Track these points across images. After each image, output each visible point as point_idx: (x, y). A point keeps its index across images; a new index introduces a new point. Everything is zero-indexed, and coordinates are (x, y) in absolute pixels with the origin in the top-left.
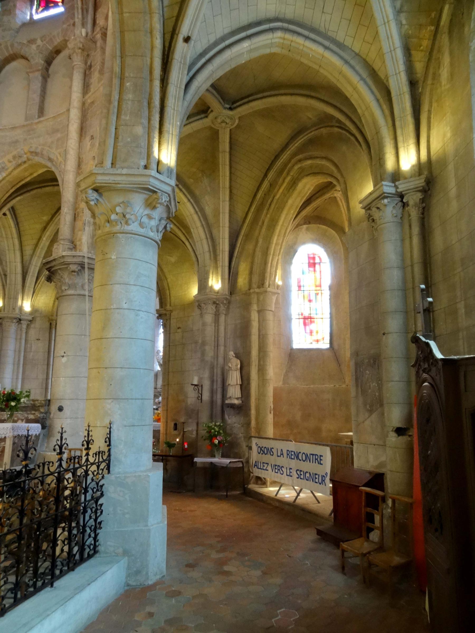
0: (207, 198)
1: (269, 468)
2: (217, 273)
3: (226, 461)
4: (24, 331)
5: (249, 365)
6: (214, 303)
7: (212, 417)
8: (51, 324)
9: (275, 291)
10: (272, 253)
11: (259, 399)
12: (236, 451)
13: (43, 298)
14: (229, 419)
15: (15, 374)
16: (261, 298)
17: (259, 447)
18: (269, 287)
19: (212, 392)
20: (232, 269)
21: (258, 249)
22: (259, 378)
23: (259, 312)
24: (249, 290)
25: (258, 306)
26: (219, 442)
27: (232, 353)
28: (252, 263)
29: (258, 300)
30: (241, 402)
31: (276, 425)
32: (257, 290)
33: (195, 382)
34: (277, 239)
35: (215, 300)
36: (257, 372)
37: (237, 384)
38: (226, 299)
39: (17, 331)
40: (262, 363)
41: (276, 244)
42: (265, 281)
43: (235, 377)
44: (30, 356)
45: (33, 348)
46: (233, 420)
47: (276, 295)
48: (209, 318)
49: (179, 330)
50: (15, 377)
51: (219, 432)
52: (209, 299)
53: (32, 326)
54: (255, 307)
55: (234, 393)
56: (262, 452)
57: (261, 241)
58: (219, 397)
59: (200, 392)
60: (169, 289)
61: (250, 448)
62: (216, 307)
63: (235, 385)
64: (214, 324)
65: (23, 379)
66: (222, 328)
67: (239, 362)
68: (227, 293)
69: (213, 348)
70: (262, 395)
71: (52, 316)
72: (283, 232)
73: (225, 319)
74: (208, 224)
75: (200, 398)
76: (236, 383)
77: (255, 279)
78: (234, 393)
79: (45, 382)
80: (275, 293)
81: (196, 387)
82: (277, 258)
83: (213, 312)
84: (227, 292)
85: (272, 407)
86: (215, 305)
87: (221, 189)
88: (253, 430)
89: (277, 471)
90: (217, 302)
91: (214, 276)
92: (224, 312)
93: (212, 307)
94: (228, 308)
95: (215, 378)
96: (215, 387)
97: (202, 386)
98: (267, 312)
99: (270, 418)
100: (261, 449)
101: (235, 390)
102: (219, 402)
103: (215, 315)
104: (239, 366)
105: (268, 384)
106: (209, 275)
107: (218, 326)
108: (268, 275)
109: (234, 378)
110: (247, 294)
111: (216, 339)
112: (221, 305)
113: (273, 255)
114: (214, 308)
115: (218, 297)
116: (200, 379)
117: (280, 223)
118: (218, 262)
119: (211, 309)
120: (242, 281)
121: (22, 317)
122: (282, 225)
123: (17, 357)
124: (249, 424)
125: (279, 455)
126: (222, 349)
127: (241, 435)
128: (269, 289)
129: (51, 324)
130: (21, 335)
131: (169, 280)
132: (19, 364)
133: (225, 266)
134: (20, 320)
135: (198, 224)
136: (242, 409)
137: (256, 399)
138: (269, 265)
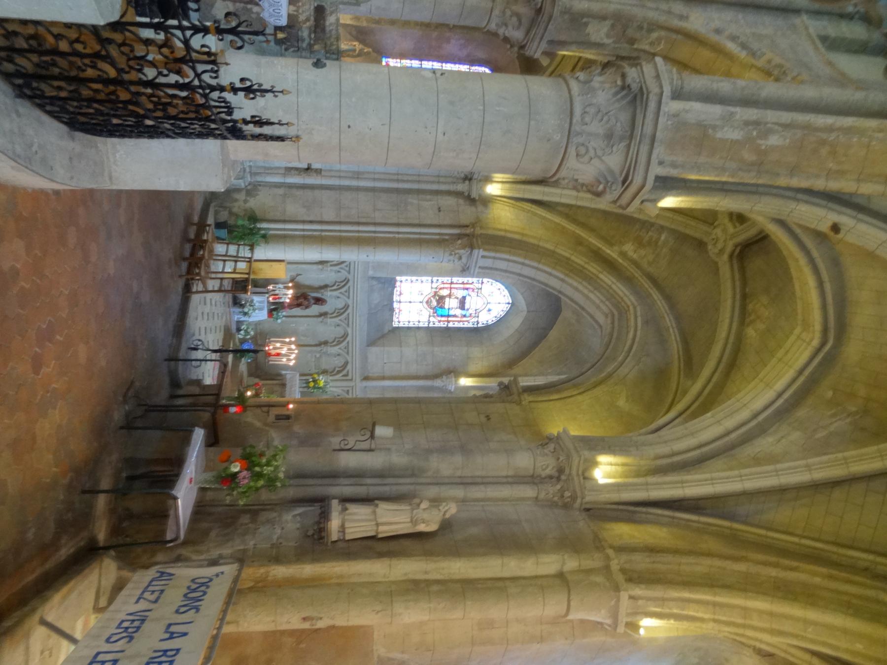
0: (796, 435)
1: (143, 605)
3: (184, 496)
4: (452, 188)
5: (429, 554)
6: (561, 471)
7: (300, 475)
8: (467, 226)
9: (623, 619)
10: (718, 599)
11: (339, 585)
12: (213, 534)
13: (508, 214)
14: (295, 516)
15: (382, 176)
16: (599, 579)
17: (211, 580)
18: (631, 597)
19: (357, 475)
20: (644, 509)
21: (717, 563)
22: (394, 582)
23: (561, 576)
24: (611, 547)
25: (572, 572)
26: (235, 475)
27: (452, 509)
28: (676, 552)
29: (589, 571)
30: (334, 537)
31: (273, 639)
32: (615, 565)
34: (761, 612)
35: (567, 471)
36: (411, 577)
37: (377, 525)
38: (574, 498)
39: (451, 177)
40: (435, 588)
41: (745, 609)
42: (643, 586)
43: (396, 519)
44: (412, 199)
45: (426, 204)
46: (291, 523)
47: (609, 621)
48: (523, 461)
49: (483, 419)
50: (376, 176)
51: (259, 475)
52: (569, 457)
53: (461, 201)
54: (571, 563)
55: (356, 522)
56: (194, 586)
57: (741, 567)
60: (560, 399)
61: (214, 563)
63: (376, 519)
64: (511, 473)
65: (373, 190)
66: (505, 492)
67: (433, 527)
68: (588, 499)
69: (459, 473)
70: (350, 591)
71: (481, 228)
72: (787, 627)
73: (528, 499)
74: (733, 447)
75: (343, 446)
76: (380, 520)
77: (641, 562)
78: (356, 522)
79: (369, 220)
80: (615, 616)
82: (706, 616)
83: (539, 471)
85: (320, 624)
87: (840, 455)
88: (262, 570)
89: (125, 624)
90: (563, 477)
91: (619, 469)
92: (542, 496)
93: (550, 468)
94: (553, 505)
96: (369, 481)
98: (564, 597)
99: (291, 619)
100: (203, 584)
101: (363, 521)
103: (532, 476)
104: (422, 528)
105: (379, 608)
107: (508, 483)
108: (658, 592)
109: (393, 519)
110: (599, 544)
111: (479, 480)
112: (558, 487)
113: (715, 604)
114: (548, 472)
115: (576, 478)
117: (812, 615)
119: (546, 464)
120: (623, 531)
121: (474, 182)
122: (806, 622)
124: (278, 560)
125: (173, 629)
126: (459, 492)
127: (252, 543)
128: (624, 596)
129: (467, 226)
131: (580, 398)
132: (398, 181)
133: (647, 490)
134: (470, 179)
135: (730, 423)
136: (317, 543)
137: (341, 576)
138: (686, 595)
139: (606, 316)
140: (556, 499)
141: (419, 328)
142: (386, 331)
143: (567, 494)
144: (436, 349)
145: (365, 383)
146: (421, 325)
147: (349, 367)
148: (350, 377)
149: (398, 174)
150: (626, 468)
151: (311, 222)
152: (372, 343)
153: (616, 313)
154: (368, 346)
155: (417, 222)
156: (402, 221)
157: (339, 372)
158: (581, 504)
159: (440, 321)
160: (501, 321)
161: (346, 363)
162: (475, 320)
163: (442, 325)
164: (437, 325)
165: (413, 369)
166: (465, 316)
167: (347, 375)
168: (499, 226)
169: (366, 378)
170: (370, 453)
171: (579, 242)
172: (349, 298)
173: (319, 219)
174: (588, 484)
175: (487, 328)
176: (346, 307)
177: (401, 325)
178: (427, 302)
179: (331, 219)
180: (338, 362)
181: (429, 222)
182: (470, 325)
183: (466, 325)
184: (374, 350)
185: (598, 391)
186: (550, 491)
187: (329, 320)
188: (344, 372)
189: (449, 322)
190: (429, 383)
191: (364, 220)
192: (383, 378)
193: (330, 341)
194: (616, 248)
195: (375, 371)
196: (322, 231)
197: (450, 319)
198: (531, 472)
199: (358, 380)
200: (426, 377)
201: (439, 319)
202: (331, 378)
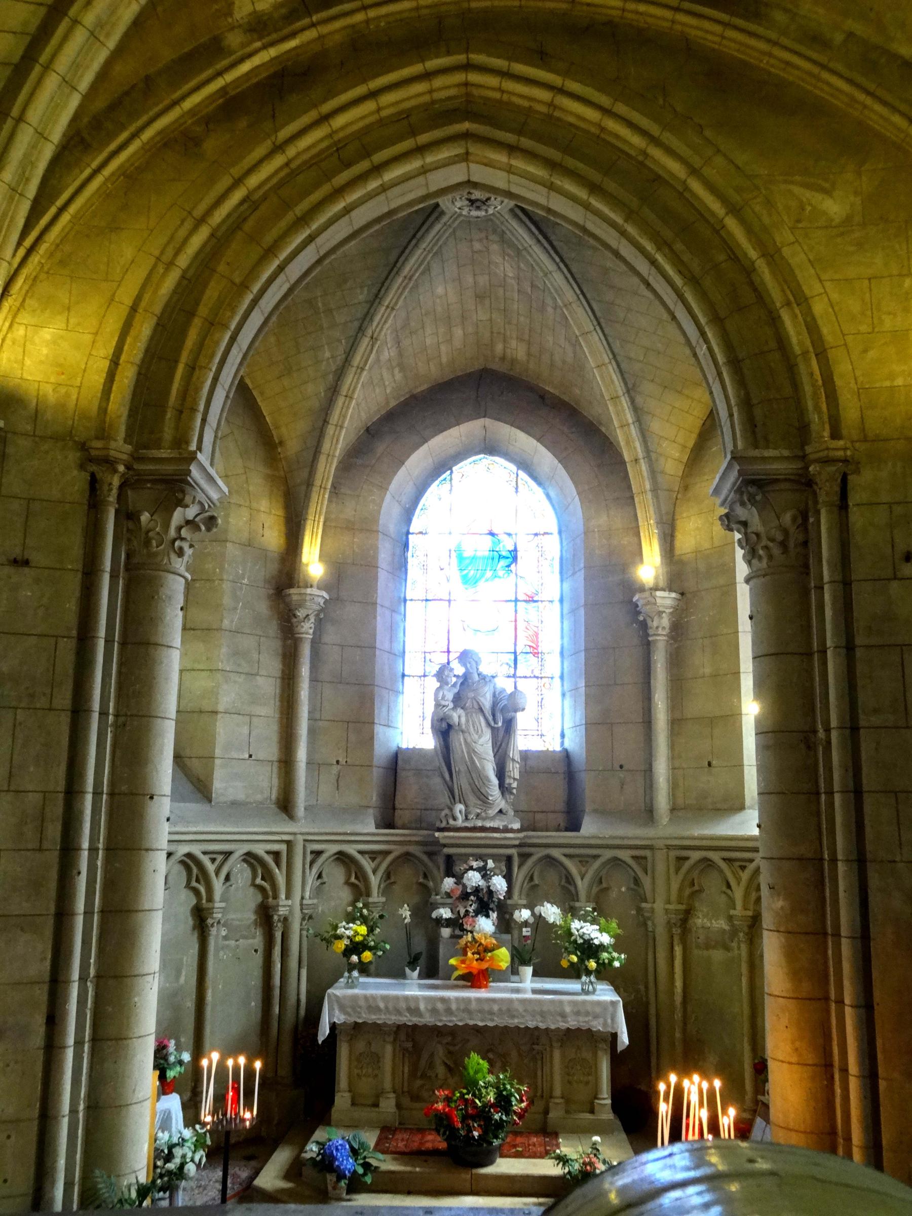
13: (47, 334)
79: (57, 809)
144: (226, 623)
145: (300, 811)
147: (260, 850)
148: (283, 848)
151: (54, 1020)
154: (209, 800)
156: (64, 698)
157: (268, 876)
165: (268, 685)
167: (276, 855)
169: (285, 805)
173: (41, 994)
179: (44, 947)
180: (242, 874)
181: (71, 606)
184: (219, 785)
188: (269, 860)
190: (306, 651)
191: (54, 831)
192: (286, 763)
195: (266, 783)
196: (83, 979)
199: (290, 827)
200: (290, 659)
202: (283, 896)
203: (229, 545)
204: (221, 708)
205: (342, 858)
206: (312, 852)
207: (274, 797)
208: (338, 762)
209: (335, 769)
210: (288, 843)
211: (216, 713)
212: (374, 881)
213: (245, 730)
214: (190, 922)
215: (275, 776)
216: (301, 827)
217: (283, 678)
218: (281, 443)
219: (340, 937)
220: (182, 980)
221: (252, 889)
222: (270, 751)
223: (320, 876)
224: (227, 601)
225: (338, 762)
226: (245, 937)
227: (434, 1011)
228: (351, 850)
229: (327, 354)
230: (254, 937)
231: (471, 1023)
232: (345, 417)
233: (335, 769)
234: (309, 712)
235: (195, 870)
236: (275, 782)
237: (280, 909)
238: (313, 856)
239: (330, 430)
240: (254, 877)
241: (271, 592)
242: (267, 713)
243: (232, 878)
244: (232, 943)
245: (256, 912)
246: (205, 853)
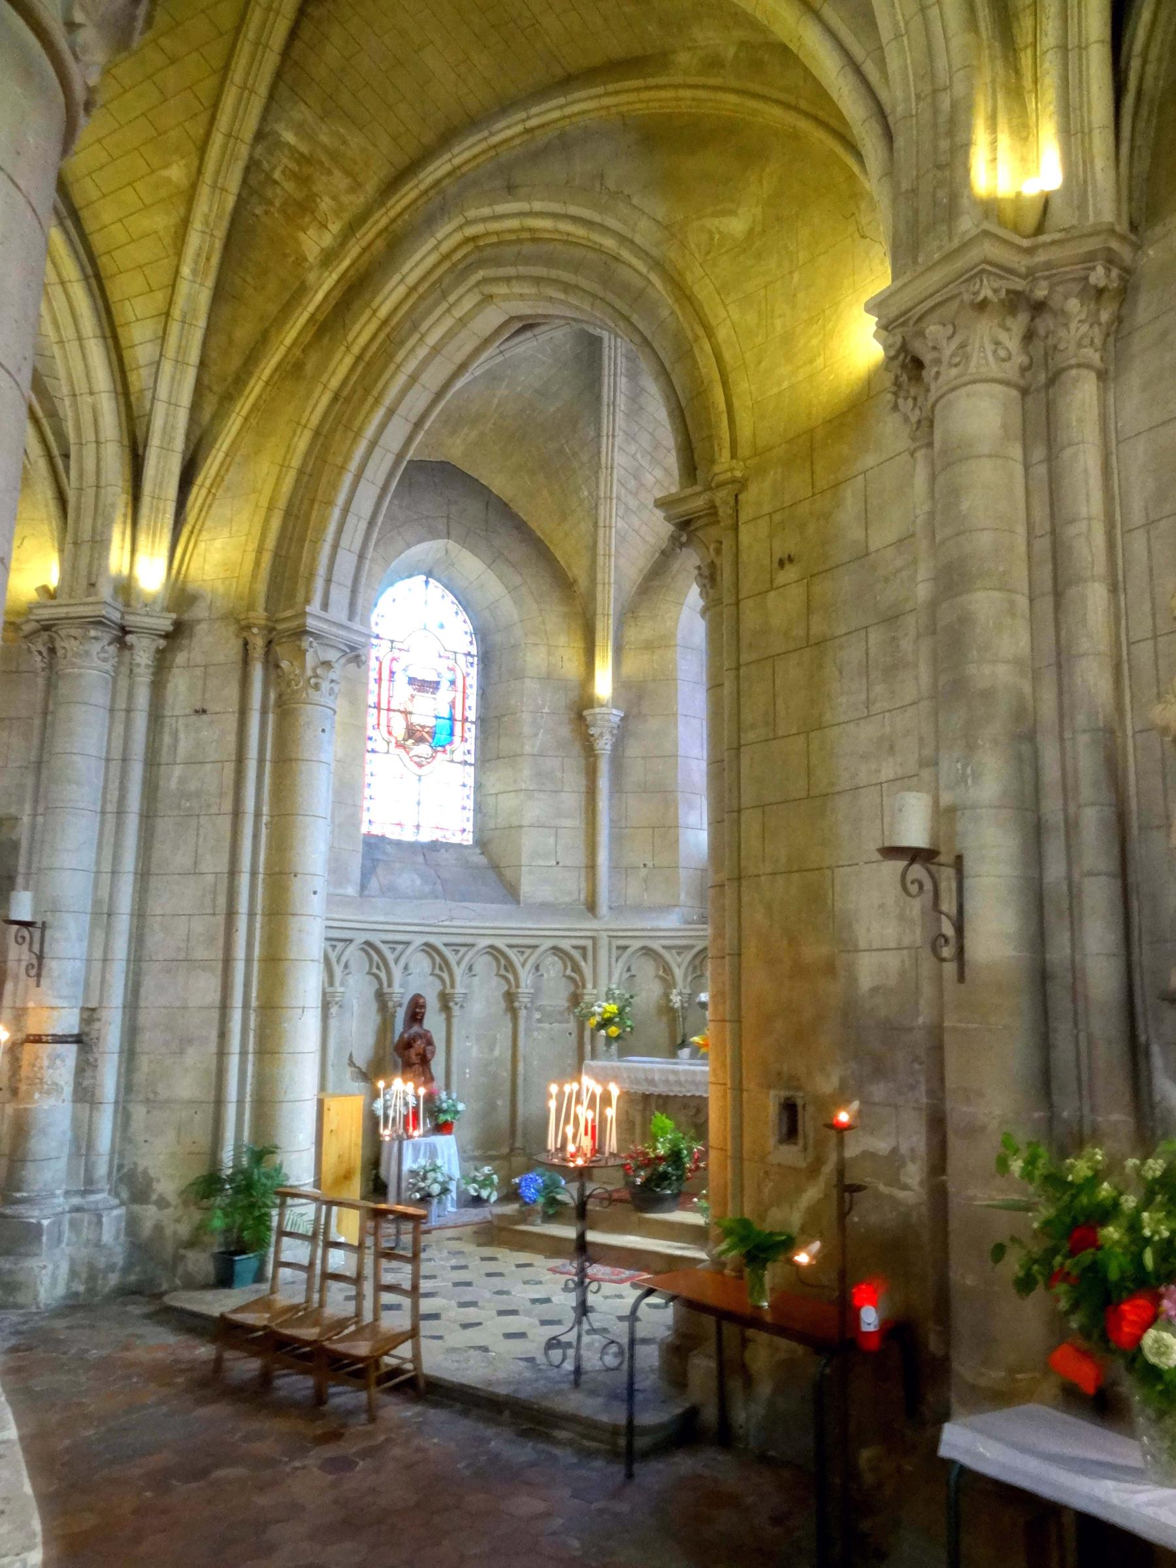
2: (1023, 131)
4: (144, 678)
6: (1014, 302)
8: (246, 644)
13: (218, 544)
15: (108, 852)
19: (1039, 907)
20: (1135, 64)
33: (915, 835)
35: (1019, 285)
39: (115, 681)
44: (172, 778)
49: (790, 573)
50: (106, 867)
53: (181, 658)
58: (1098, 938)
59: (948, 905)
60: (725, 383)
62: (1029, 336)
64: (1016, 451)
65: (143, 876)
66: (1085, 461)
68: (1108, 216)
69: (1022, 602)
71: (251, 607)
75: (947, 952)
81: (918, 871)
83: (1011, 370)
84: (1105, 207)
86: (1023, 318)
90: (1041, 293)
91: (1004, 138)
93: (1003, 336)
94: (1118, 332)
95: (1052, 807)
96: (1055, 871)
97: (959, 859)
102: (1101, 976)
103: (1025, 392)
106: (969, 128)
107: (1051, 458)
114: (1012, 342)
116: (945, 816)
118: (1026, 60)
119: (994, 346)
121: (131, 620)
123: (114, 786)
126: (1094, 598)
129: (246, 644)
130: (131, 696)
131: (722, 333)
132: (120, 813)
133: (1082, 48)
134: (124, 630)
139: (488, 298)
140: (1105, 316)
141: (479, 786)
142: (483, 860)
143: (1098, 276)
144: (528, 749)
146: (471, 782)
147: (565, 944)
148: (589, 943)
149: (103, 813)
150: (1002, 120)
151: (223, 1035)
152: (511, 892)
153: (481, 274)
154: (518, 902)
155: (230, 768)
156: (228, 806)
157: (576, 968)
158: (1123, 238)
159: (464, 739)
160: (465, 603)
161: (556, 950)
162: (461, 659)
163: (471, 735)
164: (471, 745)
165: (572, 799)
166: (453, 683)
167: (583, 949)
168: (248, 566)
169: (591, 907)
170: (969, 865)
171: (293, 371)
172: (408, 943)
173: (215, 1015)
174: (1062, 216)
175: (482, 634)
176: (429, 949)
177: (470, 826)
178: (420, 765)
179: (215, 982)
180: (553, 969)
181: (232, 738)
182: (474, 671)
183: (473, 680)
184: (528, 887)
185: (704, 291)
186: (1078, 328)
187: (459, 989)
188: (576, 955)
189: (465, 720)
190: (604, 767)
191: (222, 901)
192: (591, 867)
193: (506, 988)
194: (311, 277)
195: (572, 887)
196: (246, 1006)
197: (458, 716)
198: (1014, 393)
199: (595, 924)
200: (591, 774)
201: (457, 738)
202: (589, 986)
203: (527, 681)
204: (525, 822)
205: (647, 951)
206: (618, 948)
207: (583, 897)
208: (645, 865)
209: (643, 872)
210: (593, 938)
211: (521, 827)
212: (678, 973)
213: (552, 841)
214: (503, 1005)
215: (583, 879)
216: (606, 921)
217: (588, 793)
218: (575, 581)
219: (593, 1014)
220: (497, 1053)
221: (564, 980)
222: (578, 858)
223: (629, 970)
224: (527, 730)
225: (645, 865)
226: (560, 1022)
227: (667, 1082)
228: (656, 945)
229: (586, 493)
230: (568, 1022)
231: (697, 1094)
232: (609, 545)
233: (643, 872)
234: (611, 821)
235: (503, 962)
236: (583, 885)
237: (586, 997)
238: (620, 952)
239: (600, 560)
240: (565, 968)
241: (573, 716)
242: (574, 823)
243: (542, 970)
244: (546, 1026)
245: (568, 1001)
246: (510, 946)
